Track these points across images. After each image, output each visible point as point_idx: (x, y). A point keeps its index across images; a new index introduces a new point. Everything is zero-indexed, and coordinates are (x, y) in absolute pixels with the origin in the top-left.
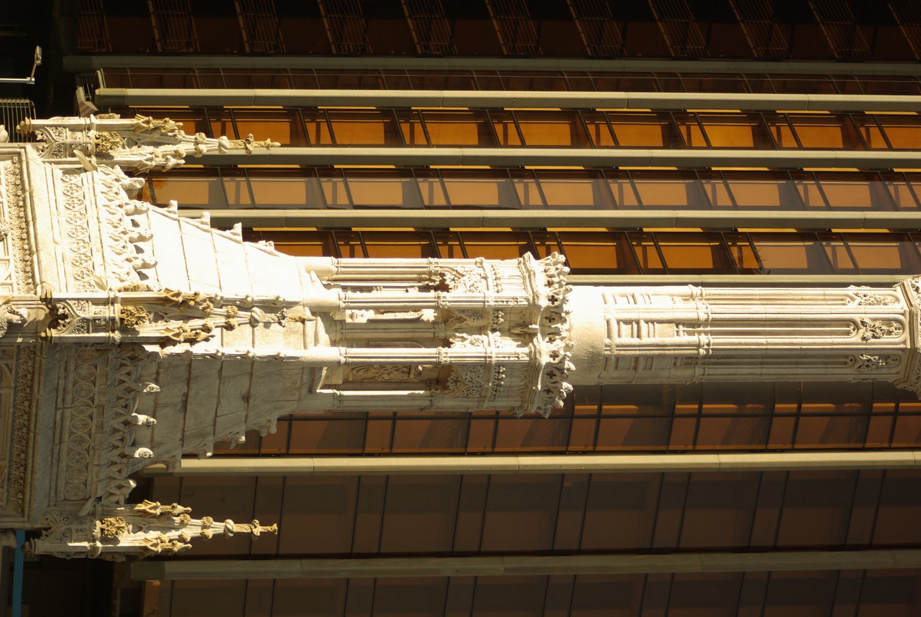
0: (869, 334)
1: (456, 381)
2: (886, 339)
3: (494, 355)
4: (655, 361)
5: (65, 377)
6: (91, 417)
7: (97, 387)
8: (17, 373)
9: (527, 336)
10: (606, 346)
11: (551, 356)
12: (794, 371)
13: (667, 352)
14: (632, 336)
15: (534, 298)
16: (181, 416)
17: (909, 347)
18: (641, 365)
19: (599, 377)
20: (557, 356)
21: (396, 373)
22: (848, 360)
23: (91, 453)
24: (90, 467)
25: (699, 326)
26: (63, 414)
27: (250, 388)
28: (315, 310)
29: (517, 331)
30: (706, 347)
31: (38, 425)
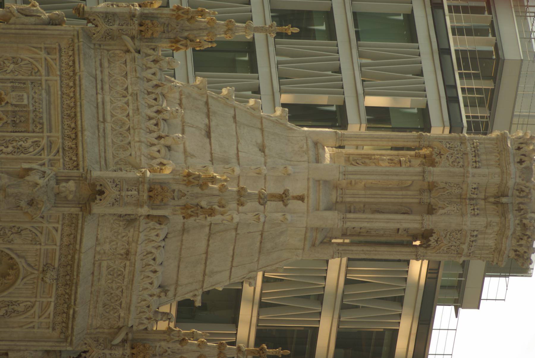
5: (102, 72)
6: (127, 103)
7: (129, 80)
8: (61, 66)
16: (208, 140)
23: (132, 131)
24: (132, 143)
26: (103, 99)
27: (263, 141)
31: (82, 91)
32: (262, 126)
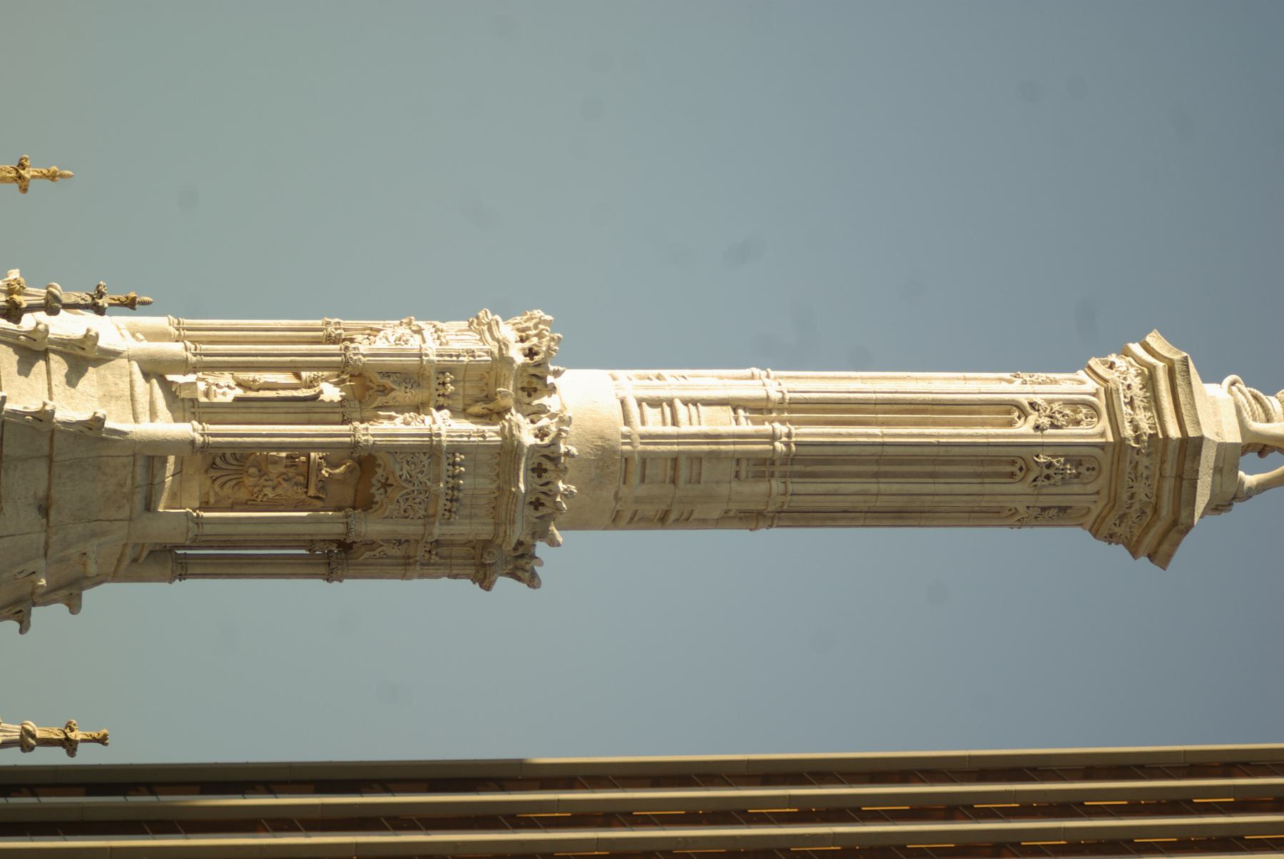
0: (1045, 421)
1: (386, 485)
2: (1072, 430)
3: (443, 432)
4: (705, 465)
9: (495, 416)
10: (624, 436)
11: (536, 436)
12: (931, 488)
13: (723, 447)
14: (664, 423)
15: (500, 349)
17: (1111, 439)
18: (684, 473)
19: (617, 498)
20: (546, 435)
21: (285, 485)
22: (1015, 469)
25: (770, 411)
27: (49, 488)
28: (147, 369)
29: (477, 409)
30: (784, 439)
32: (52, 447)
